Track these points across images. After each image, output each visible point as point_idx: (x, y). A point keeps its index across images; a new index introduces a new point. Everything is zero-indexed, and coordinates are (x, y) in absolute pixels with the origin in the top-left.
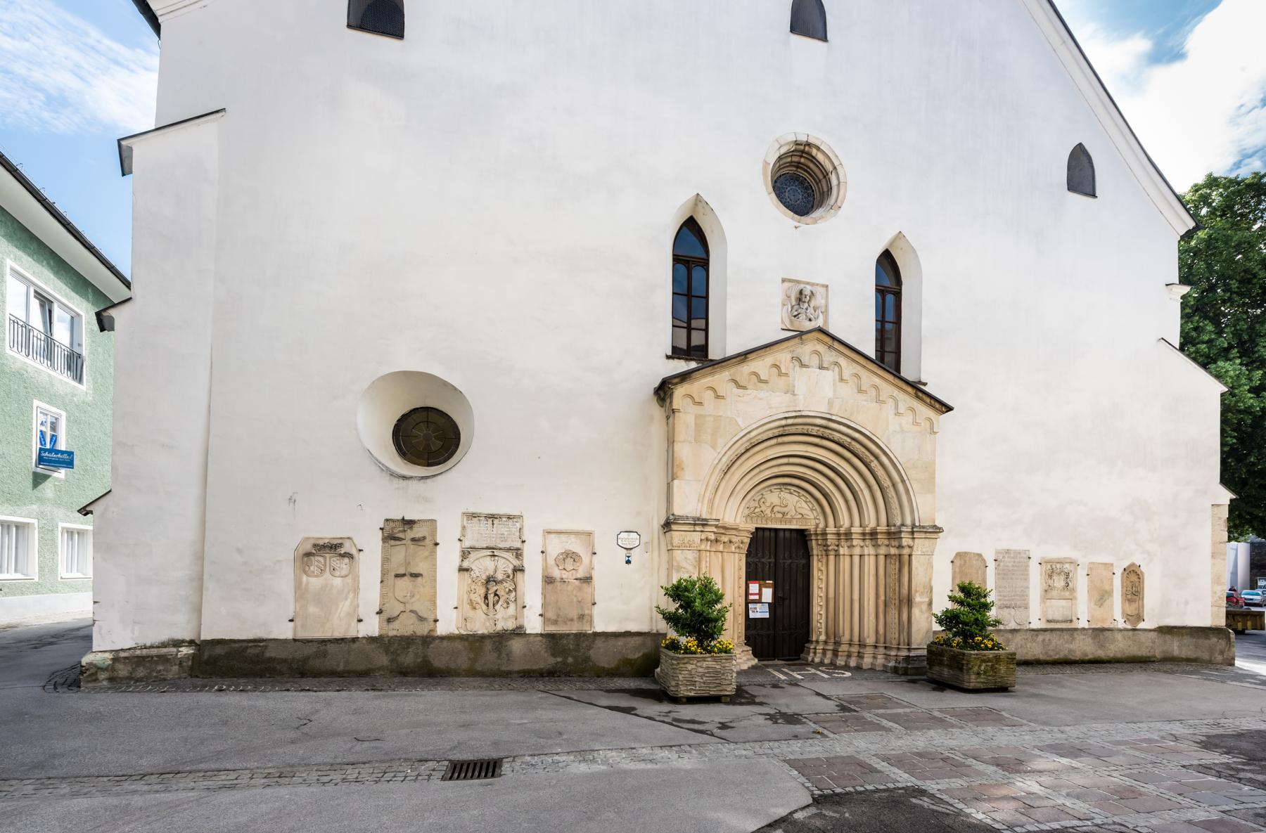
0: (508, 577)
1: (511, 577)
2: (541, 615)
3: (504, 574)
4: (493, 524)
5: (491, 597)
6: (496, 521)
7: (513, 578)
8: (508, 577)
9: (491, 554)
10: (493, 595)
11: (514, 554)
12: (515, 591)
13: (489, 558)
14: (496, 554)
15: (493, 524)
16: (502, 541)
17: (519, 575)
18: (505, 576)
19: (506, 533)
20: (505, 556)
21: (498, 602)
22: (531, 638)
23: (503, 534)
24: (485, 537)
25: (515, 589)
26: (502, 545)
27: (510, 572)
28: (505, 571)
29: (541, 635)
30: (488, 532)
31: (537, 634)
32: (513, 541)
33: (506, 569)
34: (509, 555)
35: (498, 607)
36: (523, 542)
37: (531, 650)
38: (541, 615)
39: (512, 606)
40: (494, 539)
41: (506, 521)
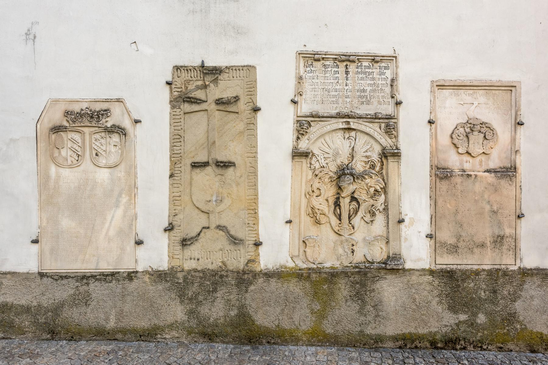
0: (373, 167)
1: (377, 169)
2: (430, 236)
3: (367, 162)
4: (347, 73)
5: (345, 202)
6: (352, 68)
7: (382, 169)
8: (373, 167)
9: (346, 126)
10: (348, 200)
11: (383, 125)
12: (385, 193)
13: (340, 134)
14: (353, 127)
15: (347, 73)
16: (362, 103)
17: (391, 163)
18: (368, 166)
19: (369, 89)
20: (368, 130)
21: (356, 211)
22: (414, 278)
23: (364, 91)
24: (334, 96)
25: (385, 190)
26: (362, 110)
27: (375, 157)
28: (367, 157)
29: (431, 272)
30: (338, 87)
31: (423, 270)
32: (379, 103)
33: (368, 154)
34: (374, 129)
35: (357, 220)
36: (398, 103)
37: (415, 299)
38: (430, 236)
39: (380, 219)
40: (348, 100)
41: (369, 67)
